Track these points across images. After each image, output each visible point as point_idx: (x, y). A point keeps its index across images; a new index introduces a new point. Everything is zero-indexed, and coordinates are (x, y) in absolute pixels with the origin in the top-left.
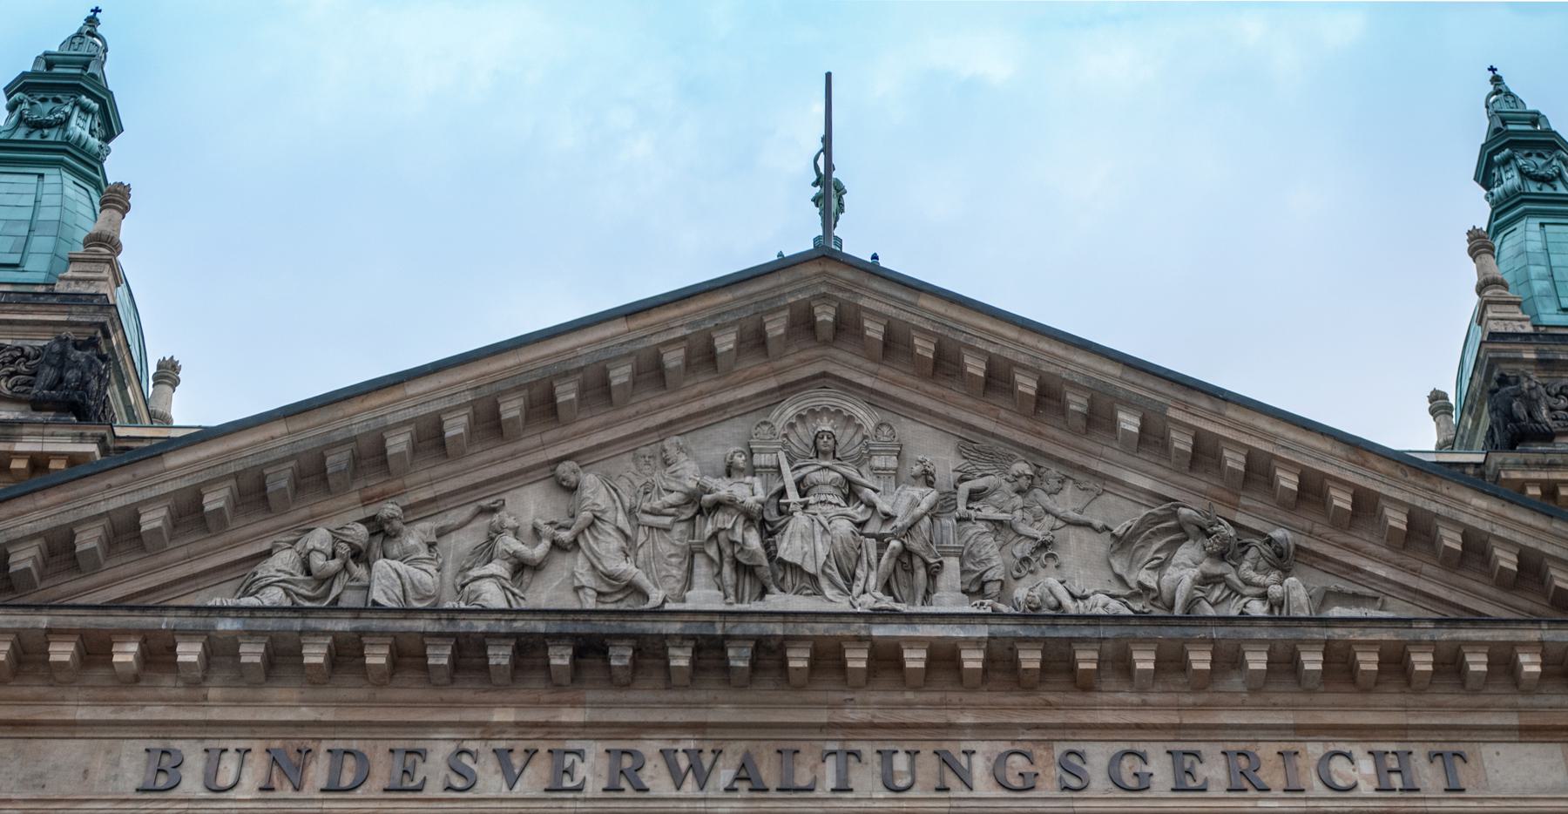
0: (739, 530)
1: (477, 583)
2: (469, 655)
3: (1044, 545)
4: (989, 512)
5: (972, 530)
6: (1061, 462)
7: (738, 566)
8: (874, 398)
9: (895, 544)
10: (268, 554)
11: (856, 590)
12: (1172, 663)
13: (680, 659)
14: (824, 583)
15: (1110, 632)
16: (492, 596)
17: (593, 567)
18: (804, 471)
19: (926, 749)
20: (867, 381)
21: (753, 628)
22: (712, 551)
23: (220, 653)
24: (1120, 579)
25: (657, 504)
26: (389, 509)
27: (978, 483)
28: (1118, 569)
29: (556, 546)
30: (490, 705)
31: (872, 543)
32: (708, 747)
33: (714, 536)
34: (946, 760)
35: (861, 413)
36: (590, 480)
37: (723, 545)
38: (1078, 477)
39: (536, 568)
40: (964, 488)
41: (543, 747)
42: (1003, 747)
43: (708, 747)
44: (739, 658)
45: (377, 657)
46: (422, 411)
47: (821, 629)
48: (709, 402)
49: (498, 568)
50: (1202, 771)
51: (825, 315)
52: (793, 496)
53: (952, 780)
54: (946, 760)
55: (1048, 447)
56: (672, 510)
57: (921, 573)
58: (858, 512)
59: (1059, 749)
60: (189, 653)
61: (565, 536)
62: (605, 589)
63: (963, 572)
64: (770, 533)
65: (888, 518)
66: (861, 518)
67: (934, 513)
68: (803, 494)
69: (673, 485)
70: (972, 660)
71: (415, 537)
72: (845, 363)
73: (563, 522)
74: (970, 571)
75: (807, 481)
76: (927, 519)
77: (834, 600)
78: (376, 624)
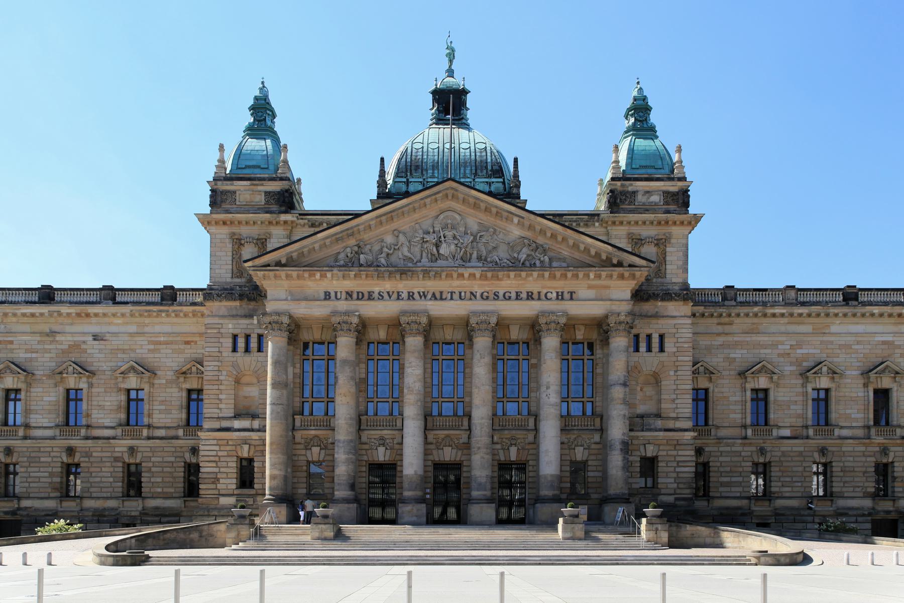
4: (484, 240)
5: (480, 245)
34: (472, 293)
49: (384, 255)
52: (443, 238)
58: (456, 242)
64: (437, 246)
67: (472, 242)
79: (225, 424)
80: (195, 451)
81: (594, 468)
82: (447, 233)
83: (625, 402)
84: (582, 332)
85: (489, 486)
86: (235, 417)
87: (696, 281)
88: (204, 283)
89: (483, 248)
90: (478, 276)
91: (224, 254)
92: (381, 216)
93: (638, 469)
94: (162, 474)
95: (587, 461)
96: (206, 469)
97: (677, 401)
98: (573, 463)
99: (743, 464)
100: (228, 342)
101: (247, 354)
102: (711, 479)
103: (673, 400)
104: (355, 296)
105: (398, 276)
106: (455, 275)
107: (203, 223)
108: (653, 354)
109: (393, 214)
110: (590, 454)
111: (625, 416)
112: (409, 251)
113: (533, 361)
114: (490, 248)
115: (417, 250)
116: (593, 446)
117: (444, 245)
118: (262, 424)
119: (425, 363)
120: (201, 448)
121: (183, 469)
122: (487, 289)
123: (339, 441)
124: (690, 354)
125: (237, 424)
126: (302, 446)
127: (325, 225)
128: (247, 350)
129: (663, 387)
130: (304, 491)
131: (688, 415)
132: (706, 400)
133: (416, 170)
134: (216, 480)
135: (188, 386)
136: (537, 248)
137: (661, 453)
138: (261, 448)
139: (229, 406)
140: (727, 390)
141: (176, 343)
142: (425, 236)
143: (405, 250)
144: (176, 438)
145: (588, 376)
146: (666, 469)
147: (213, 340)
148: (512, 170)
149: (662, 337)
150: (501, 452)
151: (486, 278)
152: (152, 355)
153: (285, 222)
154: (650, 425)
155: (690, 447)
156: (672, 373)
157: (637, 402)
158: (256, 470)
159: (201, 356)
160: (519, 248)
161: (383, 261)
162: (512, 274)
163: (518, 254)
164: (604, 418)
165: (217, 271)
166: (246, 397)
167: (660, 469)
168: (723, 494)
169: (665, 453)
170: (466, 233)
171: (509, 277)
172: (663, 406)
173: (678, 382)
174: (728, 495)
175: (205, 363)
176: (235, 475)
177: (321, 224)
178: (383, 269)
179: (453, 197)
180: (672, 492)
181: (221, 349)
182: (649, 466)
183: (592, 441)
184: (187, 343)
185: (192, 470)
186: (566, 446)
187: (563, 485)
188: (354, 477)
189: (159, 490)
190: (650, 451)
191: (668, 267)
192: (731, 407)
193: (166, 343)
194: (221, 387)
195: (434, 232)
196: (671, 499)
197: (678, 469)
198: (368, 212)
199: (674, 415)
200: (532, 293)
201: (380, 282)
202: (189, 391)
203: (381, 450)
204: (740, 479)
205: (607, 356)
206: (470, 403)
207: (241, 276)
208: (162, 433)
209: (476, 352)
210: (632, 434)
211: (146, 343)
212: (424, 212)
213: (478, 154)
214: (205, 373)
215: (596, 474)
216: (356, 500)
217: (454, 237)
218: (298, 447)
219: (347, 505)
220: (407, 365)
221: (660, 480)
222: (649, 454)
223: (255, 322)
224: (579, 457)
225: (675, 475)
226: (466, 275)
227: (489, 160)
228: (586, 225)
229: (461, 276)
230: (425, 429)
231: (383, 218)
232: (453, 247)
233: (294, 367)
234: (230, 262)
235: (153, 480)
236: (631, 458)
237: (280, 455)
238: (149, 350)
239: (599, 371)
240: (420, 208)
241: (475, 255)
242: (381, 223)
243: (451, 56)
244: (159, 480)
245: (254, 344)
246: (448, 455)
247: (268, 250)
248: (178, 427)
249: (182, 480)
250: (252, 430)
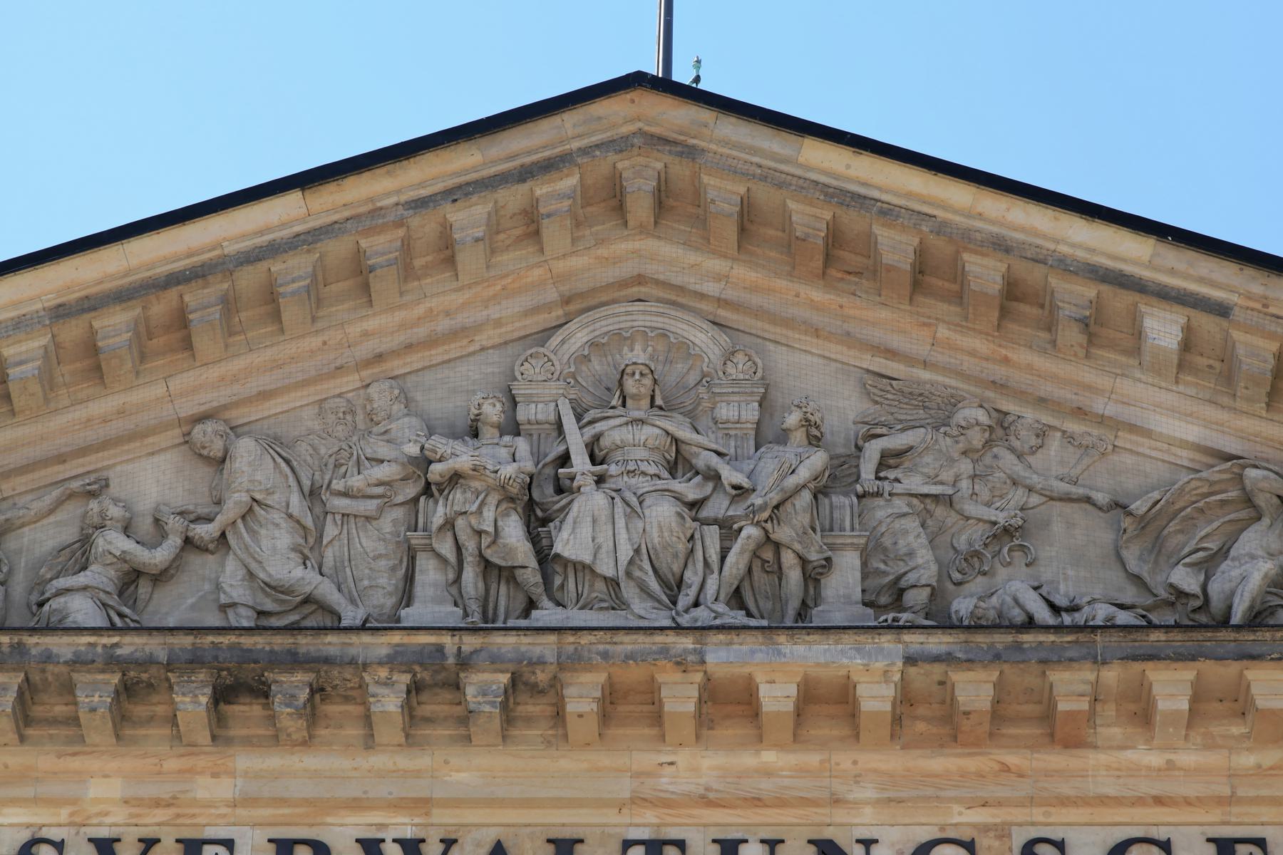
0: (489, 514)
1: (62, 600)
3: (1008, 531)
4: (914, 483)
5: (880, 511)
6: (1042, 402)
7: (487, 566)
9: (751, 532)
11: (683, 601)
14: (629, 590)
17: (251, 575)
18: (599, 427)
22: (446, 548)
24: (1137, 579)
25: (356, 481)
28: (1133, 566)
31: (712, 536)
33: (449, 525)
37: (462, 537)
38: (1073, 427)
40: (873, 450)
52: (580, 461)
56: (380, 490)
58: (691, 490)
61: (204, 531)
62: (269, 606)
63: (865, 576)
64: (538, 521)
65: (740, 491)
66: (692, 496)
69: (383, 450)
73: (202, 511)
74: (878, 572)
75: (605, 442)
76: (806, 496)
82: (614, 432)
90: (876, 697)
92: (91, 304)
105: (193, 702)
106: (680, 697)
109: (194, 296)
112: (309, 548)
115: (369, 549)
117: (590, 502)
122: (964, 819)
151: (951, 727)
160: (1207, 533)
161: (82, 610)
162: (1171, 686)
163: (1209, 564)
170: (766, 435)
171: (1141, 713)
178: (63, 646)
179: (663, 200)
195: (513, 428)
201: (42, 758)
212: (440, 300)
217: (678, 461)
226: (777, 696)
229: (730, 705)
231: (115, 325)
232: (662, 513)
240: (407, 272)
241: (845, 580)
242: (94, 364)
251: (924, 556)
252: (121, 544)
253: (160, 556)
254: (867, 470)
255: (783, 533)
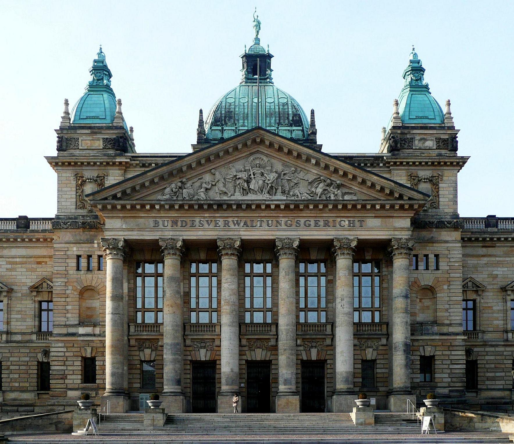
2: (201, 206)
4: (287, 178)
5: (284, 181)
7: (243, 189)
8: (267, 155)
10: (165, 188)
12: (316, 206)
13: (234, 207)
14: (257, 192)
15: (305, 202)
16: (202, 196)
19: (274, 220)
20: (266, 152)
21: (246, 202)
23: (162, 206)
25: (229, 177)
26: (184, 180)
27: (285, 172)
29: (212, 185)
30: (204, 214)
32: (239, 220)
34: (277, 222)
35: (265, 158)
36: (217, 173)
39: (209, 189)
40: (283, 173)
41: (213, 220)
42: (287, 219)
43: (239, 220)
44: (244, 207)
45: (186, 207)
46: (188, 163)
47: (257, 202)
48: (237, 157)
50: (319, 223)
51: (258, 140)
52: (252, 176)
53: (278, 225)
54: (277, 222)
55: (298, 165)
57: (274, 190)
58: (263, 178)
59: (296, 220)
60: (157, 207)
61: (214, 183)
64: (248, 182)
65: (269, 180)
67: (277, 179)
68: (254, 175)
70: (282, 207)
71: (188, 185)
72: (262, 148)
77: (259, 197)
78: (185, 202)
79: (72, 330)
80: (46, 353)
81: (382, 366)
83: (406, 311)
84: (370, 253)
85: (294, 381)
86: (79, 324)
87: (464, 212)
88: (52, 213)
89: (286, 184)
91: (69, 189)
93: (419, 367)
94: (18, 372)
95: (375, 360)
96: (55, 368)
97: (449, 311)
98: (364, 362)
99: (505, 362)
100: (73, 263)
101: (89, 272)
102: (479, 374)
103: (447, 310)
104: (179, 224)
107: (50, 163)
108: (429, 272)
110: (378, 354)
111: (407, 322)
112: (225, 186)
113: (330, 278)
114: (292, 184)
116: (381, 348)
117: (253, 181)
118: (103, 330)
119: (239, 280)
120: (52, 349)
121: (36, 367)
123: (167, 344)
124: (461, 271)
125: (81, 330)
126: (136, 348)
127: (153, 165)
128: (88, 269)
129: (438, 299)
130: (138, 385)
131: (459, 322)
132: (474, 309)
133: (229, 120)
134: (64, 377)
135: (39, 299)
136: (332, 184)
137: (437, 353)
138: (102, 350)
139: (74, 315)
140: (491, 301)
141: (30, 263)
142: (237, 174)
143: (220, 185)
144: (31, 341)
145: (377, 290)
146: (442, 366)
147: (60, 261)
148: (309, 120)
149: (437, 256)
150: (304, 353)
152: (10, 273)
153: (120, 163)
154: (428, 330)
155: (461, 348)
156: (445, 287)
157: (417, 311)
158: (97, 368)
159: (50, 274)
164: (390, 324)
165: (63, 204)
166: (88, 308)
167: (436, 367)
168: (489, 387)
169: (440, 353)
170: (271, 171)
172: (439, 314)
173: (450, 295)
174: (493, 387)
175: (54, 280)
176: (80, 372)
177: (150, 164)
180: (447, 385)
181: (68, 268)
182: (427, 364)
183: (380, 343)
184: (39, 263)
185: (44, 369)
186: (358, 348)
187: (356, 380)
188: (180, 374)
189: (17, 384)
190: (429, 351)
191: (440, 199)
192: (495, 315)
193: (21, 263)
194: (68, 300)
196: (446, 391)
197: (451, 366)
198: (190, 155)
199: (448, 322)
200: (328, 222)
202: (40, 302)
203: (203, 351)
204: (503, 374)
205: (392, 273)
206: (277, 312)
207: (84, 207)
208: (18, 338)
209: (281, 270)
210: (413, 338)
211: (4, 263)
213: (281, 107)
214: (54, 288)
215: (384, 371)
216: (182, 393)
218: (133, 349)
219: (174, 397)
220: (223, 281)
221: (437, 375)
222: (427, 354)
223: (96, 245)
224: (369, 357)
225: (449, 371)
227: (290, 112)
228: (372, 165)
230: (240, 334)
233: (129, 283)
234: (74, 196)
235: (11, 376)
236: (412, 358)
237: (118, 356)
238: (7, 269)
239: (385, 285)
243: (258, 26)
244: (16, 376)
245: (94, 263)
246: (259, 355)
247: (106, 186)
248: (32, 333)
249: (35, 376)
250: (94, 335)
251: (288, 187)
252: (206, 186)
253: (209, 187)
254: (282, 176)
255: (273, 185)
